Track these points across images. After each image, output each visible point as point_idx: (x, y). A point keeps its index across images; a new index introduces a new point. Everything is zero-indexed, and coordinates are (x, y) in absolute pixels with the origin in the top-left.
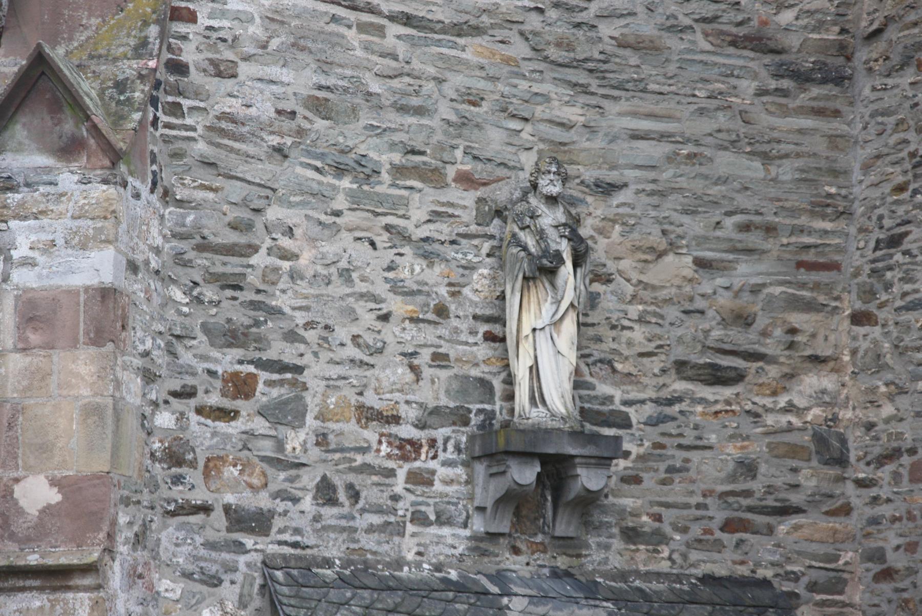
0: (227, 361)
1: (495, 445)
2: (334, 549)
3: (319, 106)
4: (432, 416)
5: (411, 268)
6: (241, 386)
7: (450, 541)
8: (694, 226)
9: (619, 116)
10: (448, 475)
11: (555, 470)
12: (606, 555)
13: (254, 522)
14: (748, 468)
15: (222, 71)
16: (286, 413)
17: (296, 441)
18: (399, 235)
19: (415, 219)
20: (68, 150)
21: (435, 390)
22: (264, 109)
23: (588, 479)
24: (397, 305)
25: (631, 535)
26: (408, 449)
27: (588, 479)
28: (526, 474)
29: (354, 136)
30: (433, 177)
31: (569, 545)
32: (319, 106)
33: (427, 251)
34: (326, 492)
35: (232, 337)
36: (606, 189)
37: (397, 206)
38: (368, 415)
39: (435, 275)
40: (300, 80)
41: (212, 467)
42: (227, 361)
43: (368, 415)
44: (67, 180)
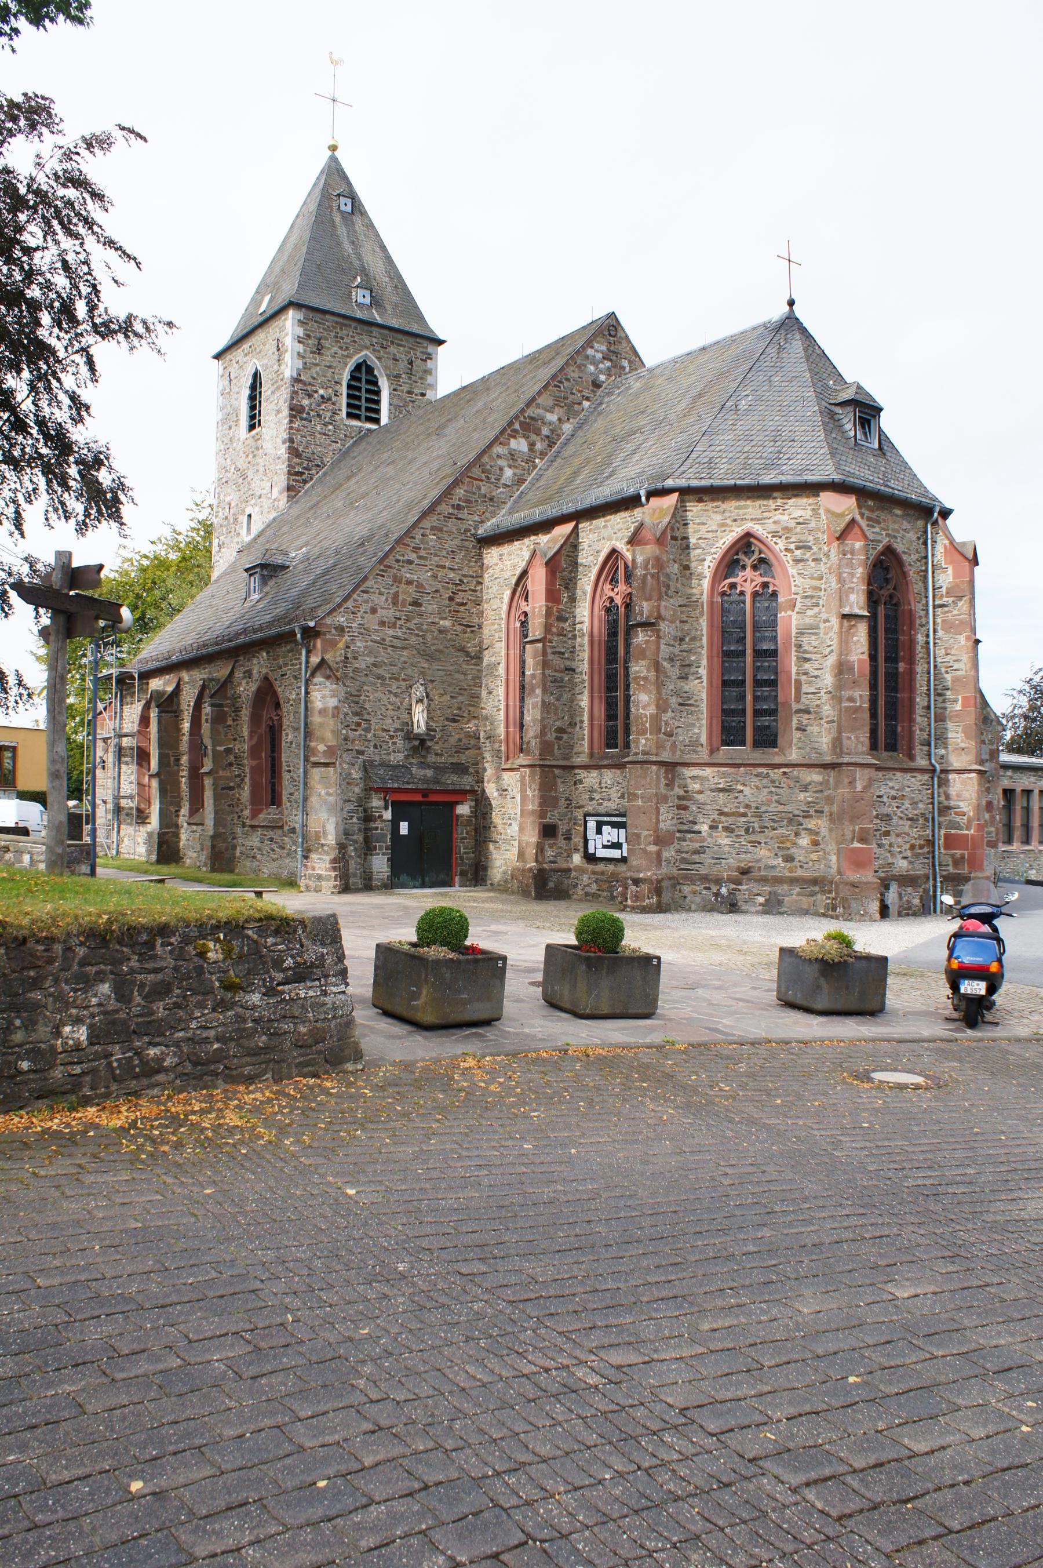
0: (356, 719)
1: (409, 736)
2: (377, 758)
3: (374, 665)
4: (397, 730)
5: (393, 699)
6: (359, 724)
7: (401, 756)
8: (450, 689)
9: (435, 666)
10: (400, 743)
11: (422, 742)
12: (431, 758)
13: (362, 753)
14: (460, 740)
15: (355, 658)
16: (367, 730)
17: (369, 736)
18: (390, 692)
19: (394, 689)
20: (328, 677)
21: (397, 725)
22: (363, 666)
23: (429, 743)
24: (390, 707)
25: (437, 754)
26: (392, 737)
27: (429, 743)
28: (417, 743)
29: (381, 671)
30: (397, 679)
31: (424, 757)
32: (374, 665)
33: (396, 695)
34: (375, 747)
35: (356, 714)
36: (432, 681)
37: (389, 685)
38: (384, 730)
39: (397, 700)
40: (370, 660)
41: (353, 741)
42: (356, 719)
43: (384, 730)
44: (328, 684)
